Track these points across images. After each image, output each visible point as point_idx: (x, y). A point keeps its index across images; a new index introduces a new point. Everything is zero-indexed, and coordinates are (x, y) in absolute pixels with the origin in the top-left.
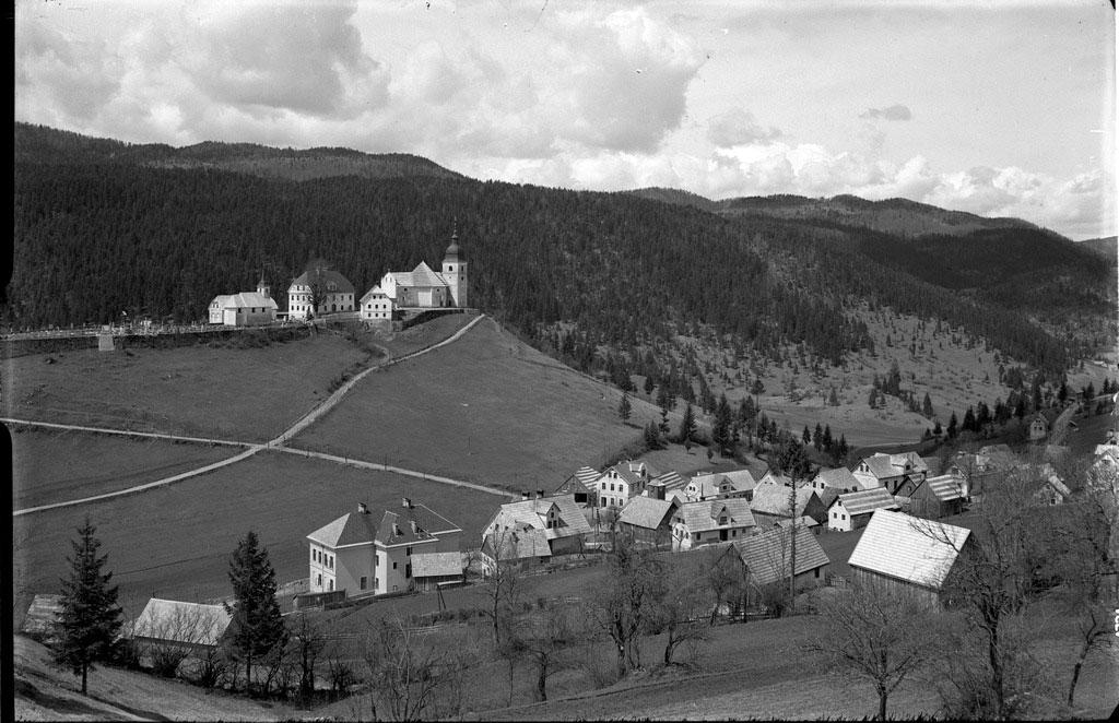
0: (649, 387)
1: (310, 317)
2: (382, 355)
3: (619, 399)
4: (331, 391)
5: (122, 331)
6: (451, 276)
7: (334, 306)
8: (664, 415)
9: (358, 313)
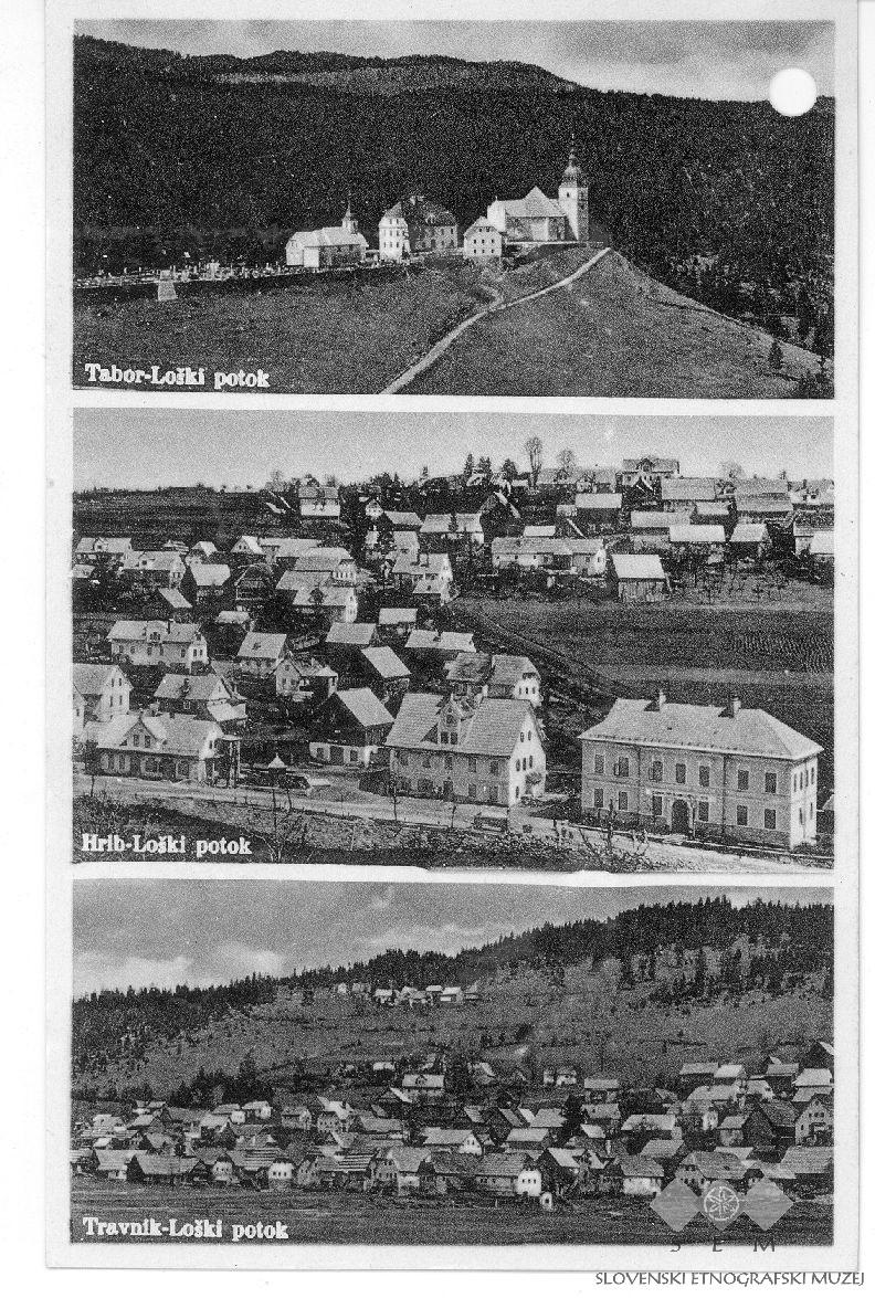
0: (803, 332)
1: (405, 255)
2: (488, 300)
3: (769, 346)
4: (433, 342)
5: (185, 276)
6: (570, 201)
7: (433, 242)
8: (821, 364)
9: (461, 249)
